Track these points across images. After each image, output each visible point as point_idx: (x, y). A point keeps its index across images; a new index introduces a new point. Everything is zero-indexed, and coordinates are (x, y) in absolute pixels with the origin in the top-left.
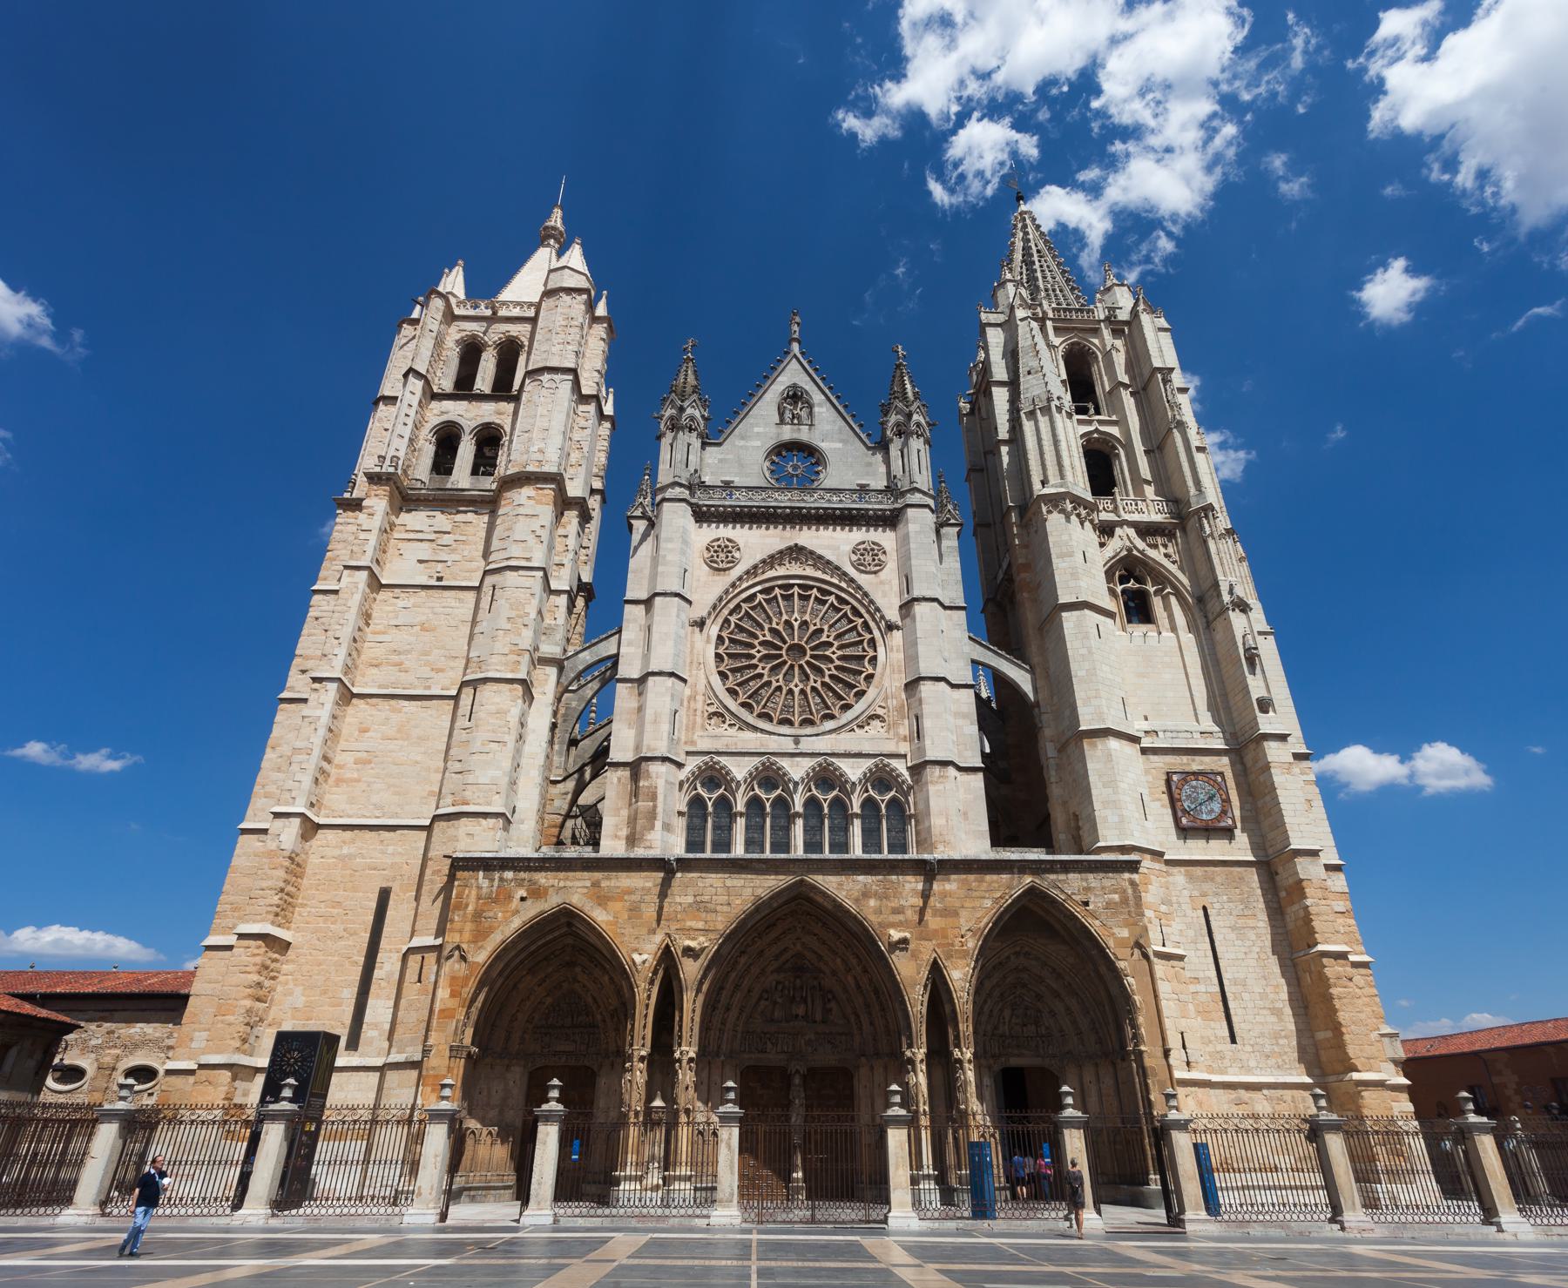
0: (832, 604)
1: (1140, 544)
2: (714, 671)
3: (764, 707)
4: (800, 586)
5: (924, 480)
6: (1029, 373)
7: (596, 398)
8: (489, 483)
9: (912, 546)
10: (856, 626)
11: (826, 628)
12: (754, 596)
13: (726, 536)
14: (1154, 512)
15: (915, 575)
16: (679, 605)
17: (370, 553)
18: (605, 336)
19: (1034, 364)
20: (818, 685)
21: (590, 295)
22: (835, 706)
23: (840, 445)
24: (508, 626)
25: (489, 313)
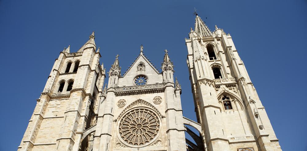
0: (148, 113)
1: (227, 89)
2: (119, 132)
3: (131, 141)
4: (140, 109)
5: (171, 80)
6: (196, 52)
7: (95, 70)
8: (69, 92)
9: (167, 96)
10: (154, 118)
11: (147, 119)
12: (129, 113)
13: (123, 99)
14: (230, 80)
15: (168, 104)
16: (110, 117)
17: (40, 110)
18: (98, 57)
19: (197, 50)
20: (144, 134)
21: (94, 49)
22: (148, 139)
23: (152, 74)
24: (68, 125)
25: (73, 55)
